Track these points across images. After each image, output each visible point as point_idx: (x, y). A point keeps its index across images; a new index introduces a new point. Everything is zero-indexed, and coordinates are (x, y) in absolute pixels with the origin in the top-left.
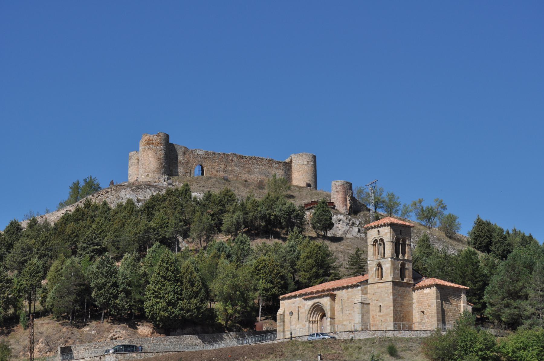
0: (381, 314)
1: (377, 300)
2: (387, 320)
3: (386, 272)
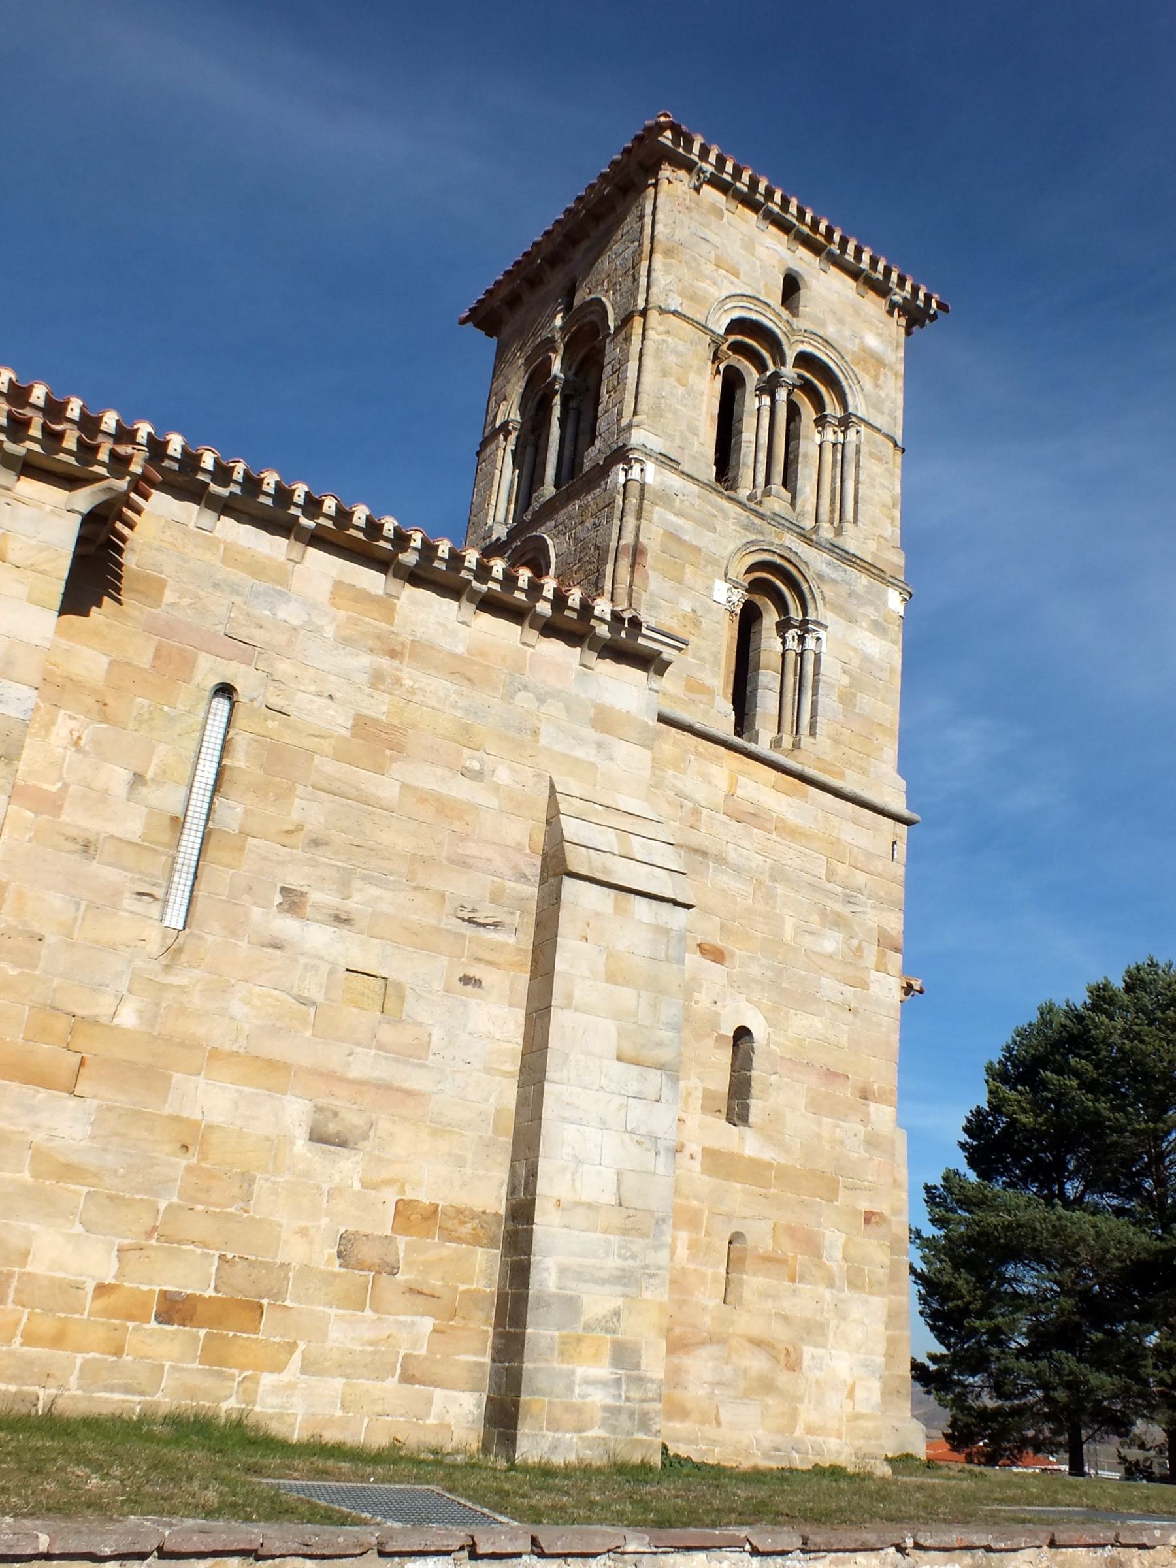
0: (747, 1143)
1: (716, 955)
2: (812, 1245)
3: (847, 699)
